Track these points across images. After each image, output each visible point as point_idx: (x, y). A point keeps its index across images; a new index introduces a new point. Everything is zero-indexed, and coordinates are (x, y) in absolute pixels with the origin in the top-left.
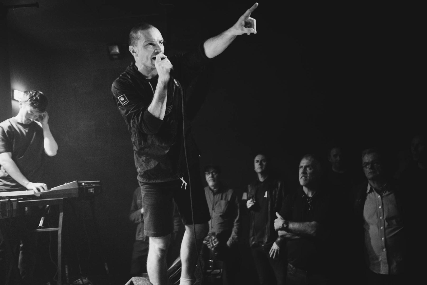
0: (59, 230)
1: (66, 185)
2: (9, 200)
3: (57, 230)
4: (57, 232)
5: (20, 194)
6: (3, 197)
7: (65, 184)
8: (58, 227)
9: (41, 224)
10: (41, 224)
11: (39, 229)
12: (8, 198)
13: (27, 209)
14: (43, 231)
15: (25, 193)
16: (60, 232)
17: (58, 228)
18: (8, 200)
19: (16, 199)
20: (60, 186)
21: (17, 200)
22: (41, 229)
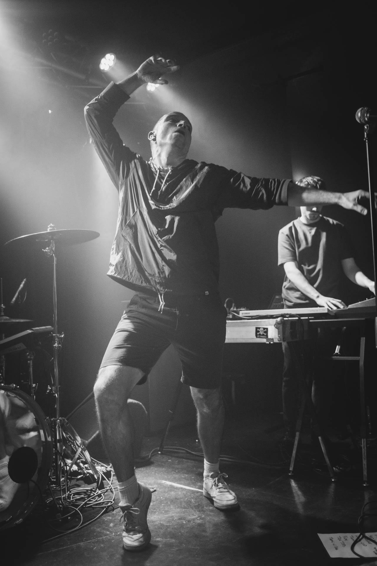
0: (361, 359)
1: (367, 301)
2: (299, 319)
3: (358, 359)
4: (358, 362)
5: (311, 311)
6: (293, 314)
7: (366, 300)
8: (359, 356)
9: (337, 349)
10: (337, 349)
11: (336, 357)
12: (298, 316)
13: (319, 329)
14: (340, 359)
15: (317, 311)
16: (362, 363)
17: (359, 357)
18: (297, 318)
19: (307, 318)
20: (360, 302)
21: (309, 318)
22: (338, 357)
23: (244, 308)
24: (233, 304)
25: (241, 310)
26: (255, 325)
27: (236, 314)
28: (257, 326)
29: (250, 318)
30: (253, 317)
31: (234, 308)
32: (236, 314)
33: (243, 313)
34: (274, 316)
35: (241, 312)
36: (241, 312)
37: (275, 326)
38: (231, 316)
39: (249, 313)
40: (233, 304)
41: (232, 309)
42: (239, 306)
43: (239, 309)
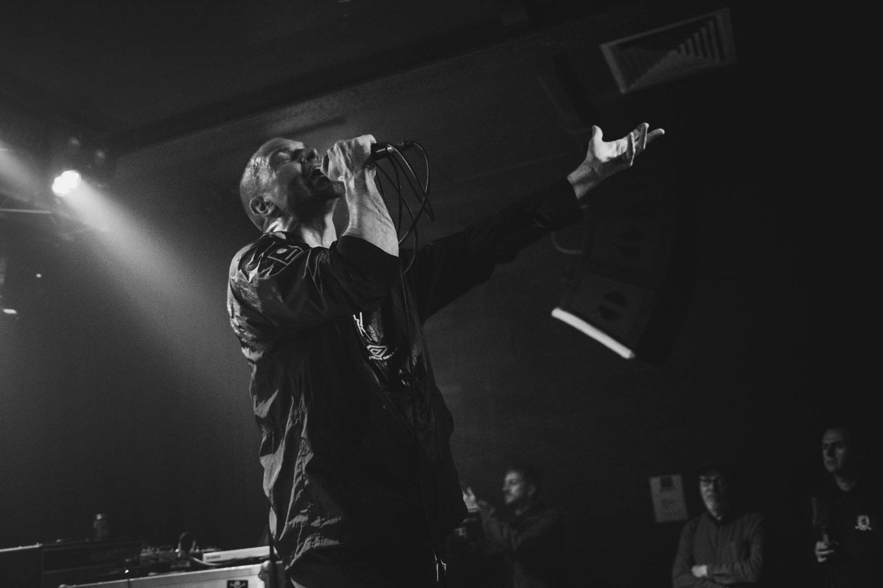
23: (213, 547)
24: (194, 543)
25: (206, 552)
26: (227, 578)
27: (196, 560)
28: (229, 577)
29: (221, 564)
30: (226, 563)
31: (195, 549)
32: (196, 560)
33: (209, 556)
34: (261, 559)
35: (205, 555)
36: (205, 555)
37: (260, 576)
38: (188, 564)
39: (218, 557)
40: (194, 543)
41: (192, 550)
42: (205, 545)
43: (203, 551)
